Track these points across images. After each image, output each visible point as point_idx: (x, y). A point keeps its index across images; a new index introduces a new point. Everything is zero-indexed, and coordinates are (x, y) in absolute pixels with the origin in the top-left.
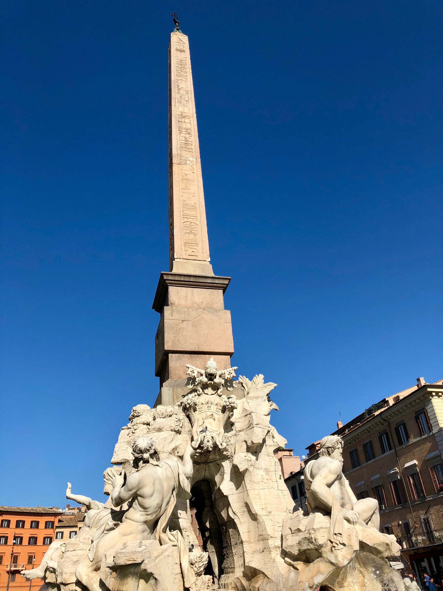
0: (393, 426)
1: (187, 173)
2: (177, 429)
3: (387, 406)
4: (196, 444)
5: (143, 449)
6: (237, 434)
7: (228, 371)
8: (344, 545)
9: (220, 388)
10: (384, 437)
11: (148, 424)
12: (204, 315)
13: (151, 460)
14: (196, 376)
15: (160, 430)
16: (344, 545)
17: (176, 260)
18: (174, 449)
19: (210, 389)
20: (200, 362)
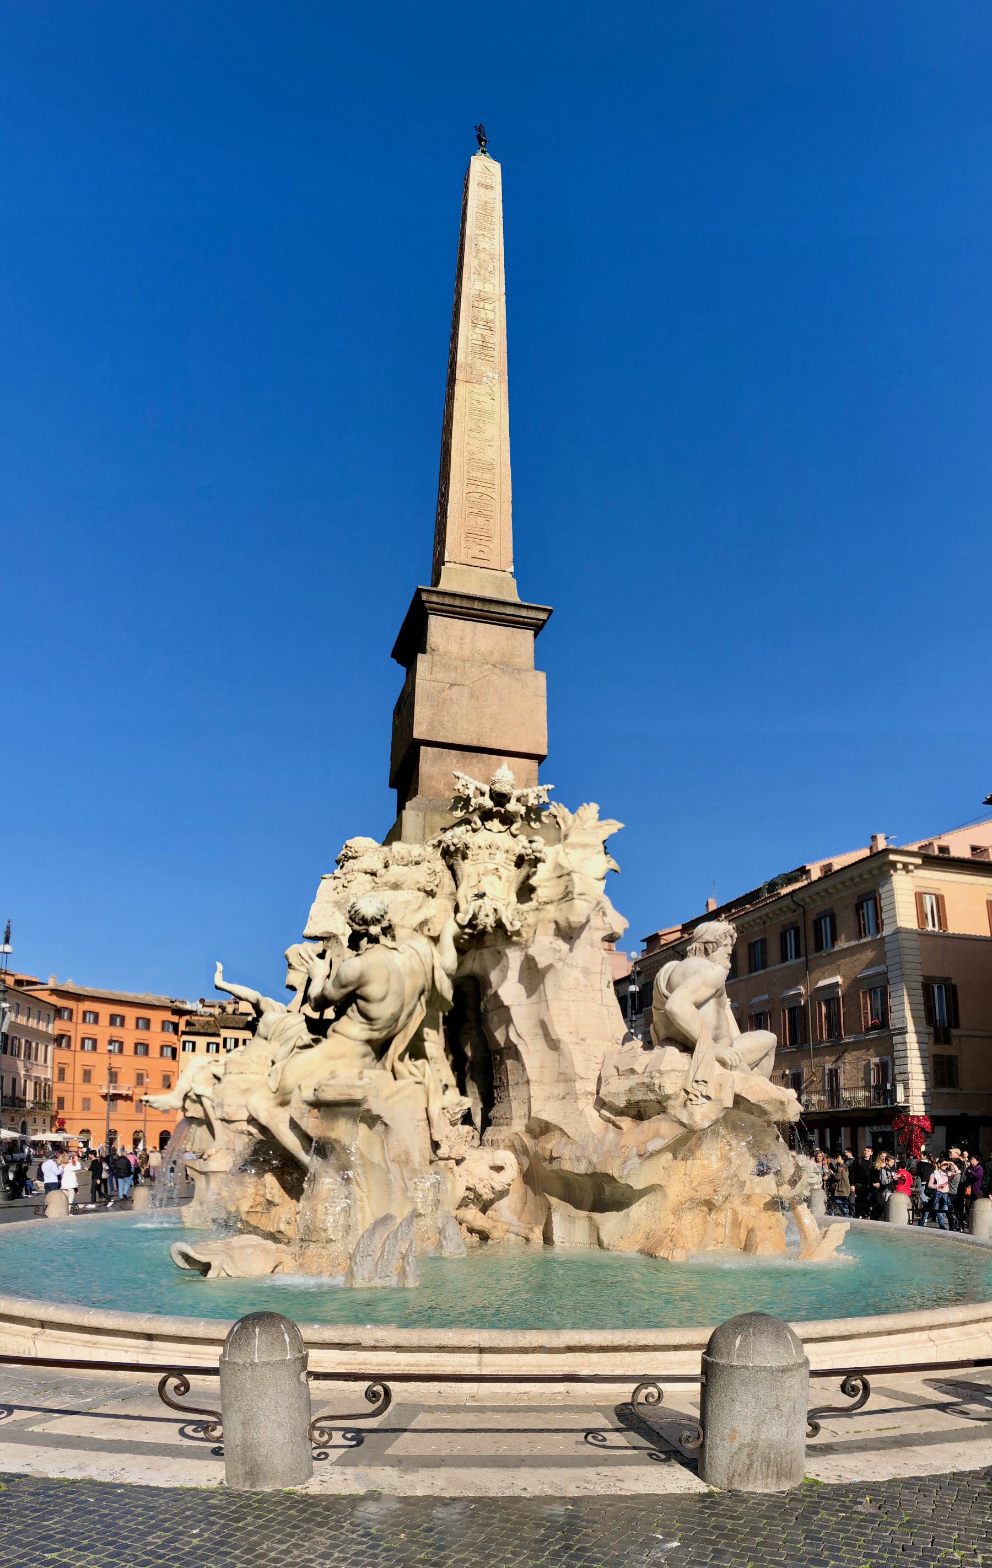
0: (812, 917)
1: (481, 398)
2: (429, 889)
3: (807, 879)
4: (464, 918)
5: (369, 918)
6: (540, 907)
7: (534, 792)
8: (708, 1098)
9: (516, 822)
10: (791, 936)
11: (373, 874)
12: (495, 678)
13: (382, 938)
14: (471, 796)
15: (396, 886)
16: (708, 1098)
17: (447, 565)
18: (423, 924)
19: (496, 821)
20: (480, 770)
